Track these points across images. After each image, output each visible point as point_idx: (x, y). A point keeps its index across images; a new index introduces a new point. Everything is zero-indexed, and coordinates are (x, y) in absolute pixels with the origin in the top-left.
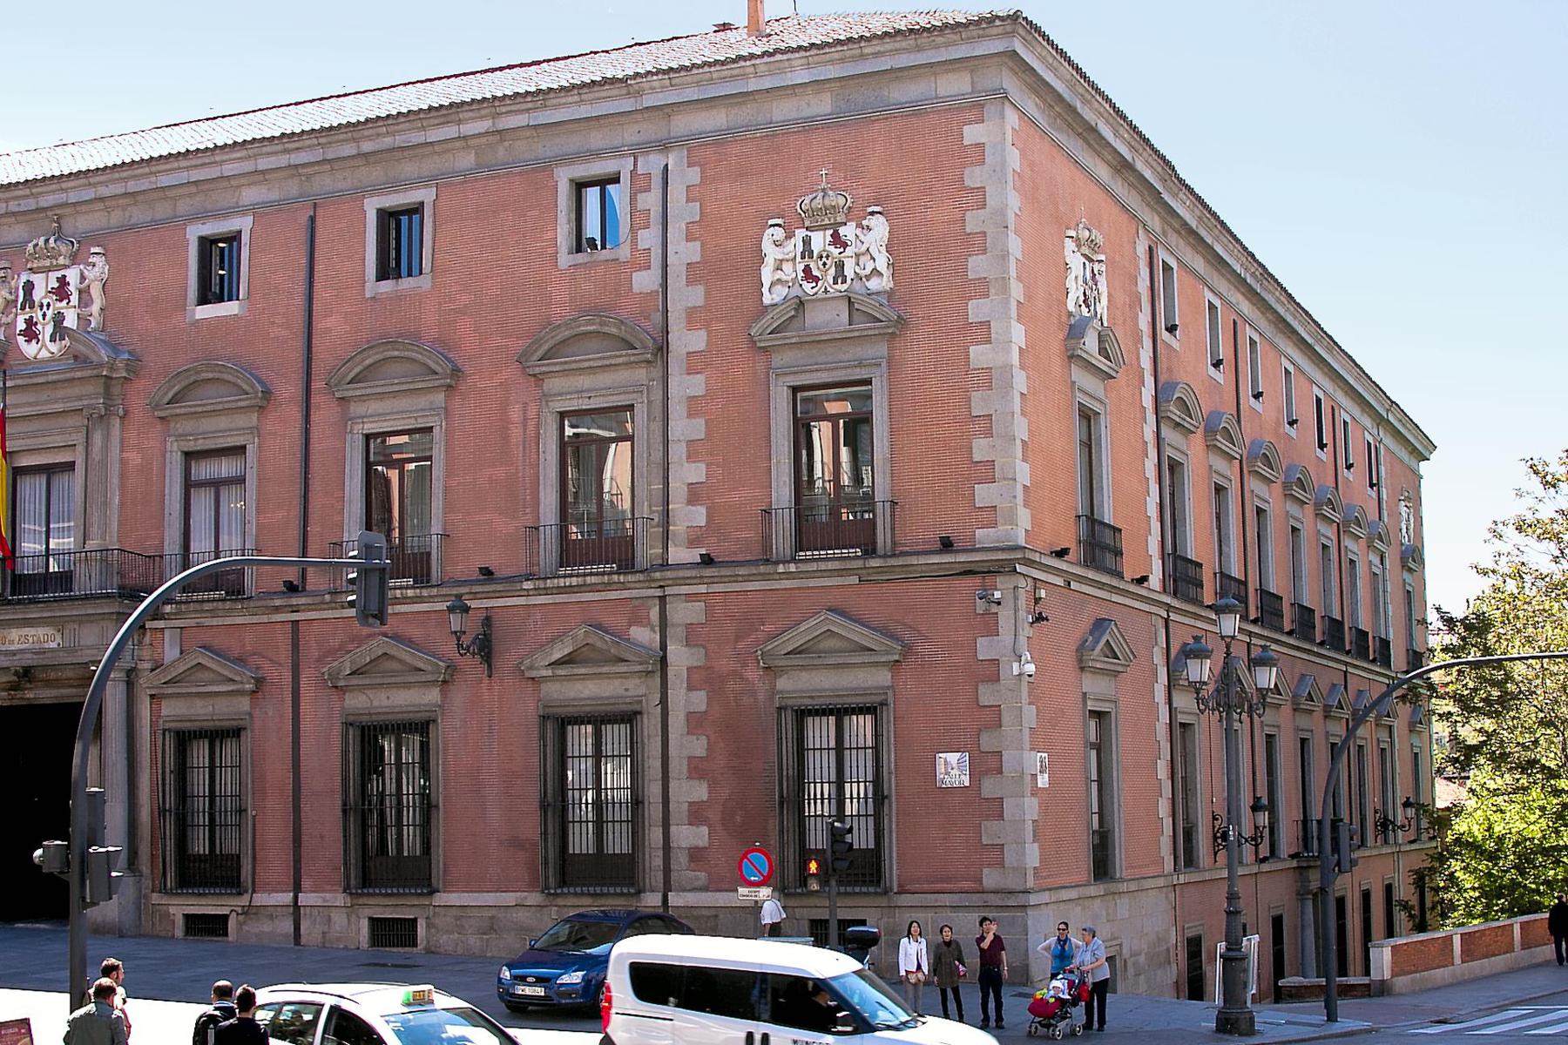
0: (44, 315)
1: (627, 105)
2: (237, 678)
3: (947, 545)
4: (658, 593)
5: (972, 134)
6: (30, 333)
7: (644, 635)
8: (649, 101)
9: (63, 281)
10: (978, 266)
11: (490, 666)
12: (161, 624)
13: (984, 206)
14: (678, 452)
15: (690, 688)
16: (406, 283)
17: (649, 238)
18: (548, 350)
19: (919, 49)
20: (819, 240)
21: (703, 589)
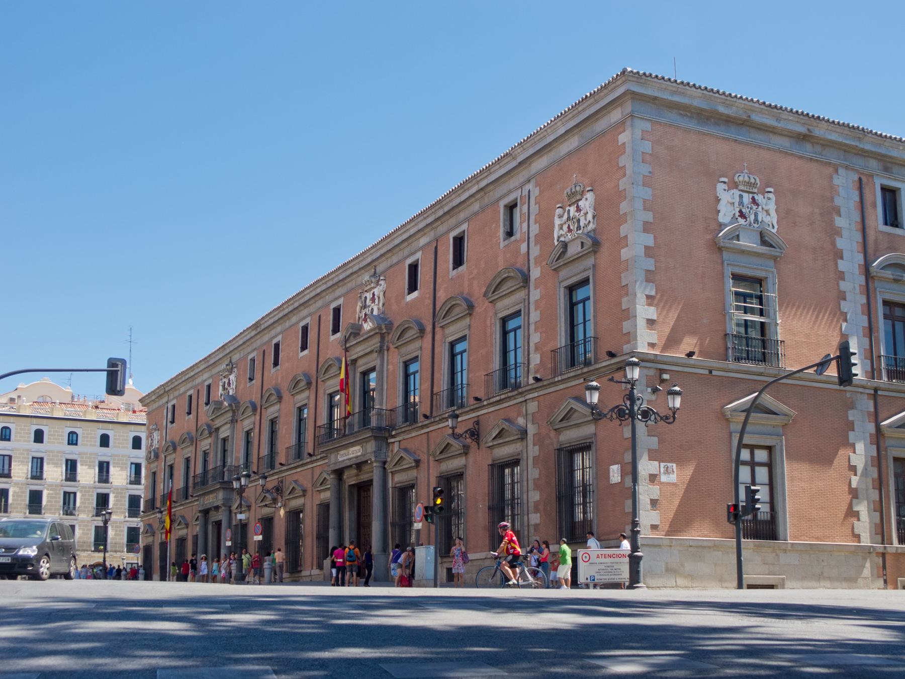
1: (514, 164)
3: (611, 355)
5: (623, 138)
6: (365, 320)
7: (521, 421)
8: (520, 159)
9: (374, 294)
10: (624, 207)
11: (478, 444)
12: (392, 440)
13: (625, 175)
14: (532, 327)
15: (534, 445)
16: (460, 268)
18: (496, 288)
19: (596, 102)
20: (573, 209)
21: (536, 395)
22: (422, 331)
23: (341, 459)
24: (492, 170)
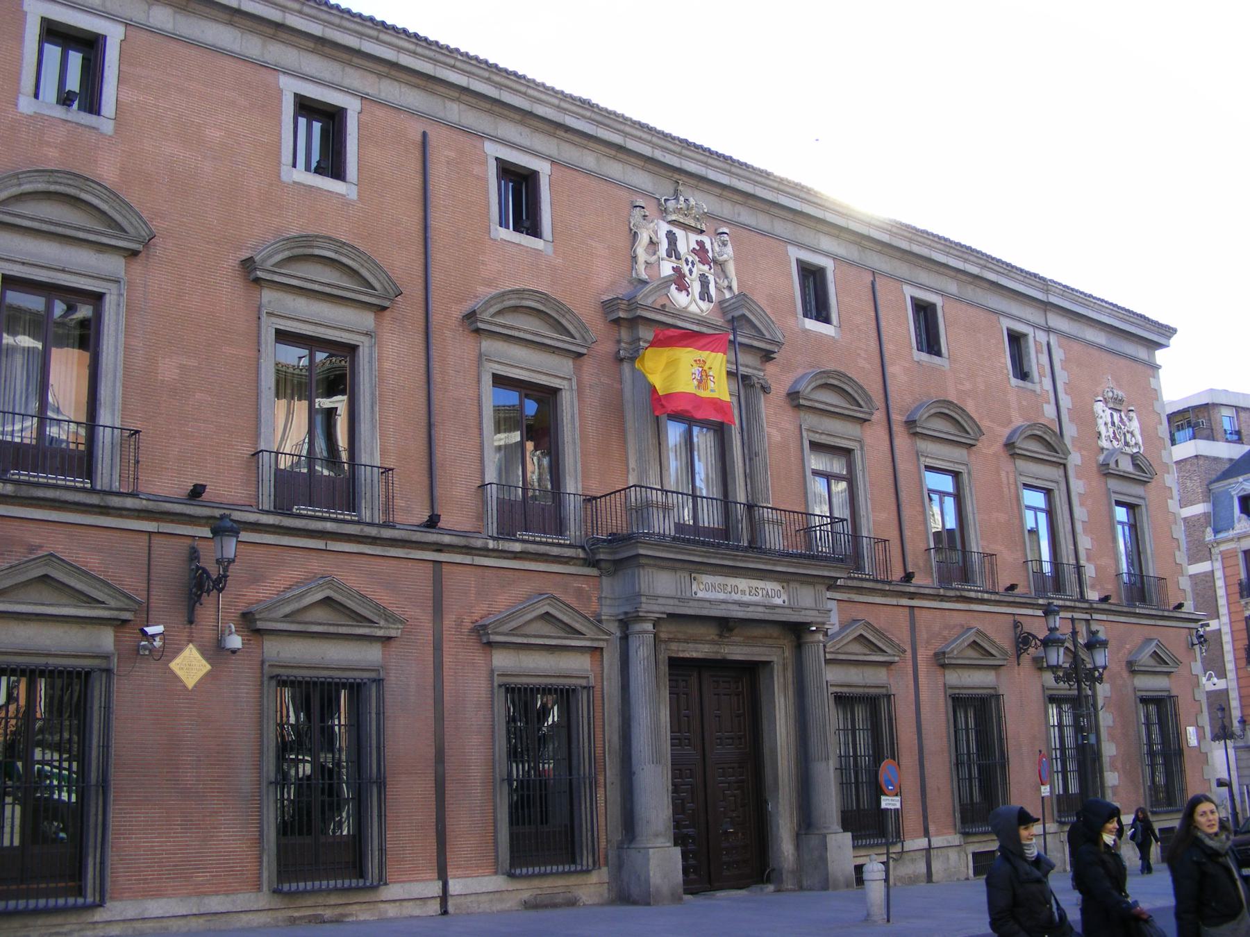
20: (1116, 416)
22: (910, 424)
23: (700, 595)
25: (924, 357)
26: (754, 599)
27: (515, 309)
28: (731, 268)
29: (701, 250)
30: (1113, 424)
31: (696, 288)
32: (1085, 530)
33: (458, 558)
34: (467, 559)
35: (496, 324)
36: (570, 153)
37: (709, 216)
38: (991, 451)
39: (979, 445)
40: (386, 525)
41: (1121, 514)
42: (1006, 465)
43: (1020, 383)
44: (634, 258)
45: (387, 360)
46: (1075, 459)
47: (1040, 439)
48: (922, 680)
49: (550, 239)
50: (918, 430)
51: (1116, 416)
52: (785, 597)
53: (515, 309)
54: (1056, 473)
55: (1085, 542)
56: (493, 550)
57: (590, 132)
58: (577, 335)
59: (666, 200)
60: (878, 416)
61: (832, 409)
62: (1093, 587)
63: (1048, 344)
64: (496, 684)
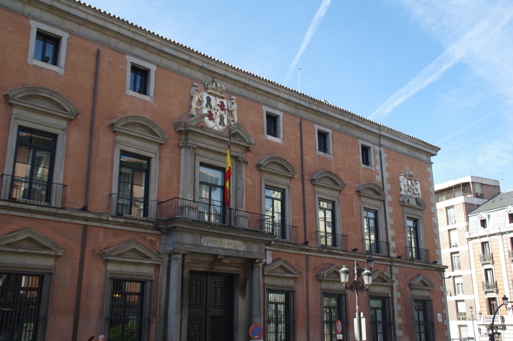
0: (216, 113)
2: (294, 272)
4: (390, 264)
15: (397, 292)
17: (378, 167)
19: (425, 147)
20: (410, 182)
21: (399, 265)
23: (205, 244)
24: (364, 122)
25: (322, 153)
26: (229, 247)
27: (134, 124)
28: (235, 113)
29: (222, 106)
30: (408, 185)
31: (218, 120)
32: (392, 228)
33: (95, 224)
34: (100, 225)
35: (123, 129)
36: (166, 62)
37: (227, 91)
38: (350, 193)
39: (344, 190)
40: (62, 208)
41: (410, 223)
42: (356, 198)
43: (365, 166)
44: (191, 107)
45: (70, 142)
46: (389, 198)
47: (373, 189)
48: (310, 285)
49: (153, 96)
50: (315, 183)
51: (410, 182)
52: (245, 248)
53: (134, 124)
54: (379, 204)
55: (391, 233)
56: (111, 221)
57: (174, 54)
58: (160, 136)
59: (208, 84)
60: (298, 176)
61: (276, 172)
62: (394, 252)
63: (380, 151)
64: (108, 277)
